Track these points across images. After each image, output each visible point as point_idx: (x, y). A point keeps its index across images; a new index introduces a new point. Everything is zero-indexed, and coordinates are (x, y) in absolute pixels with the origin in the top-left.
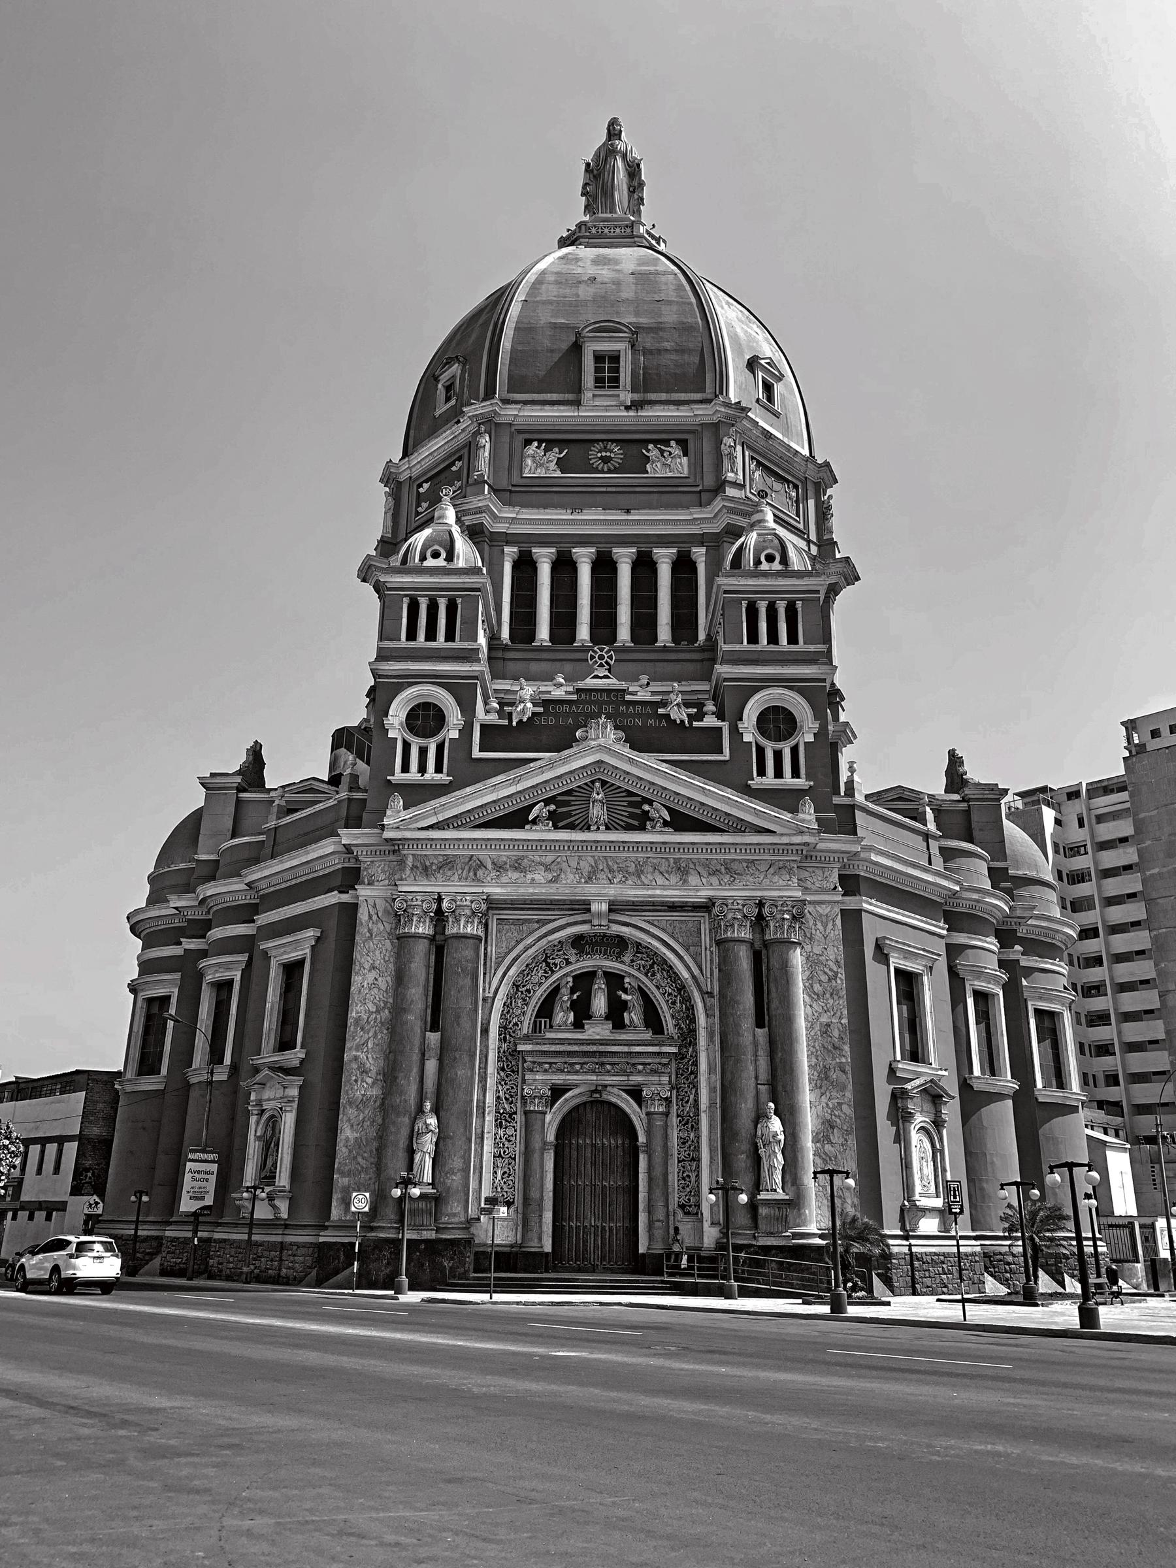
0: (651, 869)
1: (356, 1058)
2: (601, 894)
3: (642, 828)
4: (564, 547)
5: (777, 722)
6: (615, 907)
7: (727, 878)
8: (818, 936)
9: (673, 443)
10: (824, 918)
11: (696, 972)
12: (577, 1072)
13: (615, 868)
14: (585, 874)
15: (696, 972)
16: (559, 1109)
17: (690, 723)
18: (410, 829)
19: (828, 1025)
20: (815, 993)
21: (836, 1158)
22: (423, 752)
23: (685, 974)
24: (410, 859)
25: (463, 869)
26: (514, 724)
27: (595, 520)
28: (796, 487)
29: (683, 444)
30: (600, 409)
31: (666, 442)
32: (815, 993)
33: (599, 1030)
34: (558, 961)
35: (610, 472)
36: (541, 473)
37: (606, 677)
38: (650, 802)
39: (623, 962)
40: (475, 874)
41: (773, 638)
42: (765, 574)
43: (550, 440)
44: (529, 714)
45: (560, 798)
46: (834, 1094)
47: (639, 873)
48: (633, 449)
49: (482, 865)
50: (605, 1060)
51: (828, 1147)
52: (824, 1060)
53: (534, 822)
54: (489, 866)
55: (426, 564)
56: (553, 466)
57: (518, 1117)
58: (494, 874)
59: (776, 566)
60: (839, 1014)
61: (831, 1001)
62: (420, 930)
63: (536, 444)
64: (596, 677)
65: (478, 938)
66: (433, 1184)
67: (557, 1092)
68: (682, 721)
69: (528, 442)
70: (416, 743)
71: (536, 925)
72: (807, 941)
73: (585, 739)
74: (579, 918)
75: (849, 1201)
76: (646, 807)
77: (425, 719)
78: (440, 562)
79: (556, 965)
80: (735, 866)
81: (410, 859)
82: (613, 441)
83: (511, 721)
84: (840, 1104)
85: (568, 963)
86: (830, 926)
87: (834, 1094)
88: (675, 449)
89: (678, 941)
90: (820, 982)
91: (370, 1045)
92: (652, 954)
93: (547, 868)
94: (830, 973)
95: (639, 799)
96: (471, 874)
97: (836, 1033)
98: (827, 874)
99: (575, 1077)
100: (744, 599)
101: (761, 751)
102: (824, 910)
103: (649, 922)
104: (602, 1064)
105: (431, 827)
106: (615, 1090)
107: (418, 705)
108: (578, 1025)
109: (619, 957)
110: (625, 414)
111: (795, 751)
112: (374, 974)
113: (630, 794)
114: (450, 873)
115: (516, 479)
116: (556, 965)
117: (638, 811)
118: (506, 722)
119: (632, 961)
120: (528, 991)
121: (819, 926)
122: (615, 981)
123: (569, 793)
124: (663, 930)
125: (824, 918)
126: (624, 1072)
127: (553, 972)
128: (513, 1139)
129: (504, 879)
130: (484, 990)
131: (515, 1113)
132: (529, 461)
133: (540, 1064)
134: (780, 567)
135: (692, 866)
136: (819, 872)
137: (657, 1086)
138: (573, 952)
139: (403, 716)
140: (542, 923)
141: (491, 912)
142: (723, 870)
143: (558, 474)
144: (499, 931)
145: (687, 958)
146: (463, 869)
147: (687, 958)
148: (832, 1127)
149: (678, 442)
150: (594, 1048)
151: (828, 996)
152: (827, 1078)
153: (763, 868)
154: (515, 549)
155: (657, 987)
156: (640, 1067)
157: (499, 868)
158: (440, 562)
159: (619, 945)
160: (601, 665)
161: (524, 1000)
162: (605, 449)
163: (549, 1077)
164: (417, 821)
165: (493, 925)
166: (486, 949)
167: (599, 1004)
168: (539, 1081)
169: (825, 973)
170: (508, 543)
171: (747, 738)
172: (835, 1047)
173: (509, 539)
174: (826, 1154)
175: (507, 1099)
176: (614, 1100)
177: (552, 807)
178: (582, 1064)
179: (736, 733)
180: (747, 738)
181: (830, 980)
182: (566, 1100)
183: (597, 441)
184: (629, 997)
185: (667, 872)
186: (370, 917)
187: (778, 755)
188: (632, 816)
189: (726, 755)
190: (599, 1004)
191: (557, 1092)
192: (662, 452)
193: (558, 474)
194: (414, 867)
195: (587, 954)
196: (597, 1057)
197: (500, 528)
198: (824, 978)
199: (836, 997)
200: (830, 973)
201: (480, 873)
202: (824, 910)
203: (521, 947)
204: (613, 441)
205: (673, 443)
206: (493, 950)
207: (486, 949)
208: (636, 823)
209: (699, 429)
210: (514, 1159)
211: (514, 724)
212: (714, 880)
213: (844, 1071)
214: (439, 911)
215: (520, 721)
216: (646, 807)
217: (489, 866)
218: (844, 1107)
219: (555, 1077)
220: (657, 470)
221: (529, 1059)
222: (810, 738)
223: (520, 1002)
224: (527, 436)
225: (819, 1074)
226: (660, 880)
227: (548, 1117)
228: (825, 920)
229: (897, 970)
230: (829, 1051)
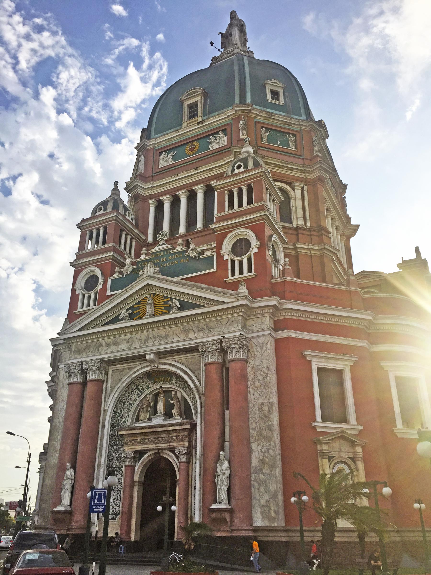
0: (172, 333)
1: (53, 444)
2: (150, 349)
3: (169, 313)
4: (173, 194)
5: (241, 246)
6: (160, 355)
7: (207, 331)
8: (258, 355)
9: (220, 132)
10: (261, 345)
11: (198, 384)
12: (146, 444)
13: (156, 336)
14: (143, 341)
15: (198, 384)
16: (141, 464)
17: (199, 257)
18: (70, 333)
19: (262, 404)
20: (256, 387)
21: (265, 482)
22: (89, 297)
23: (192, 386)
24: (74, 347)
25: (93, 348)
26: (124, 276)
27: (185, 177)
28: (294, 135)
29: (224, 131)
30: (189, 129)
31: (217, 133)
32: (256, 387)
33: (158, 421)
34: (144, 387)
35: (194, 154)
36: (166, 164)
37: (163, 244)
38: (171, 299)
39: (172, 384)
40: (98, 350)
41: (240, 204)
42: (237, 174)
43: (168, 150)
44: (130, 270)
45: (135, 306)
46: (265, 444)
47: (167, 336)
48: (204, 141)
49: (101, 345)
50: (159, 436)
51: (261, 476)
52: (260, 424)
53: (121, 320)
54: (104, 345)
55: (96, 215)
56: (170, 160)
57: (123, 469)
58: (106, 348)
59: (242, 170)
60: (268, 397)
61: (264, 391)
62: (75, 380)
63: (164, 153)
64: (160, 245)
65: (103, 382)
66: (70, 506)
67: (140, 454)
68: (195, 257)
69: (161, 153)
70: (86, 294)
71: (128, 371)
72: (252, 359)
73: (142, 275)
74: (146, 364)
75: (272, 508)
76: (170, 303)
77: (91, 283)
78: (102, 212)
79: (143, 390)
80: (211, 324)
81: (74, 347)
82: (194, 141)
83: (123, 276)
84: (268, 450)
85: (149, 388)
86: (264, 348)
87: (265, 444)
88: (221, 135)
89: (190, 370)
90: (259, 380)
91: (59, 438)
92: (183, 379)
93: (127, 341)
94: (264, 375)
95: (168, 299)
96: (96, 350)
97: (266, 408)
98: (263, 320)
99: (145, 446)
100: (226, 190)
101: (233, 262)
102: (261, 340)
103: (175, 361)
104: (157, 438)
105: (80, 330)
106: (167, 452)
107: (90, 277)
108: (150, 420)
109: (170, 381)
110: (198, 126)
111: (249, 260)
112: (63, 404)
113: (165, 297)
114: (88, 351)
115: (157, 171)
116: (143, 390)
117: (168, 305)
118: (121, 276)
119: (176, 383)
120: (131, 404)
121: (259, 349)
122: (167, 392)
123: (139, 303)
124: (183, 364)
125: (261, 345)
126: (153, 442)
127: (142, 393)
128: (120, 481)
129: (110, 350)
130: (104, 406)
131: (122, 467)
132: (161, 161)
133: (131, 441)
134: (243, 170)
135: (191, 328)
136: (259, 320)
137: (182, 447)
138: (150, 382)
139: (83, 284)
140: (130, 369)
141: (110, 367)
142: (205, 328)
143: (173, 162)
144: (112, 376)
145: (194, 377)
146: (93, 348)
147: (194, 377)
148: (264, 464)
149: (222, 131)
150: (151, 430)
151: (262, 387)
152: (261, 434)
153: (225, 322)
154: (153, 200)
155: (188, 395)
156: (174, 438)
157: (108, 345)
158: (102, 212)
159: (168, 375)
160: (162, 239)
161: (128, 409)
162: (192, 145)
163: (134, 447)
164: (72, 329)
165: (110, 373)
166: (107, 386)
167: (161, 407)
168: (129, 450)
169: (261, 375)
170: (151, 199)
171: (225, 258)
172: (265, 416)
173: (151, 197)
174: (260, 480)
175: (118, 460)
176: (166, 456)
177: (130, 311)
178: (148, 439)
179: (220, 257)
180: (225, 258)
181: (264, 379)
182: (145, 459)
183: (188, 143)
184: (172, 402)
185: (179, 333)
186: (64, 378)
187: (241, 263)
188: (165, 308)
189: (215, 269)
190: (161, 407)
191: (140, 454)
192: (216, 138)
193: (173, 162)
194: (75, 350)
195: (156, 382)
196: (154, 433)
197: (146, 193)
198: (261, 378)
199: (267, 388)
200: (264, 375)
201: (100, 349)
202: (261, 340)
203: (121, 382)
204: (194, 141)
205: (220, 132)
206: (109, 385)
207: (107, 386)
208: (167, 311)
209: (232, 122)
210: (120, 491)
211: (124, 276)
212: (201, 334)
213: (270, 430)
214: (82, 370)
215: (127, 275)
216: (170, 303)
217: (104, 345)
218: (271, 451)
219: (137, 447)
220: (214, 146)
221: (126, 439)
222: (256, 250)
223: (126, 411)
224: (160, 151)
225: (257, 432)
226: (176, 339)
227: (136, 468)
228: (262, 346)
229: (319, 369)
230: (263, 419)
